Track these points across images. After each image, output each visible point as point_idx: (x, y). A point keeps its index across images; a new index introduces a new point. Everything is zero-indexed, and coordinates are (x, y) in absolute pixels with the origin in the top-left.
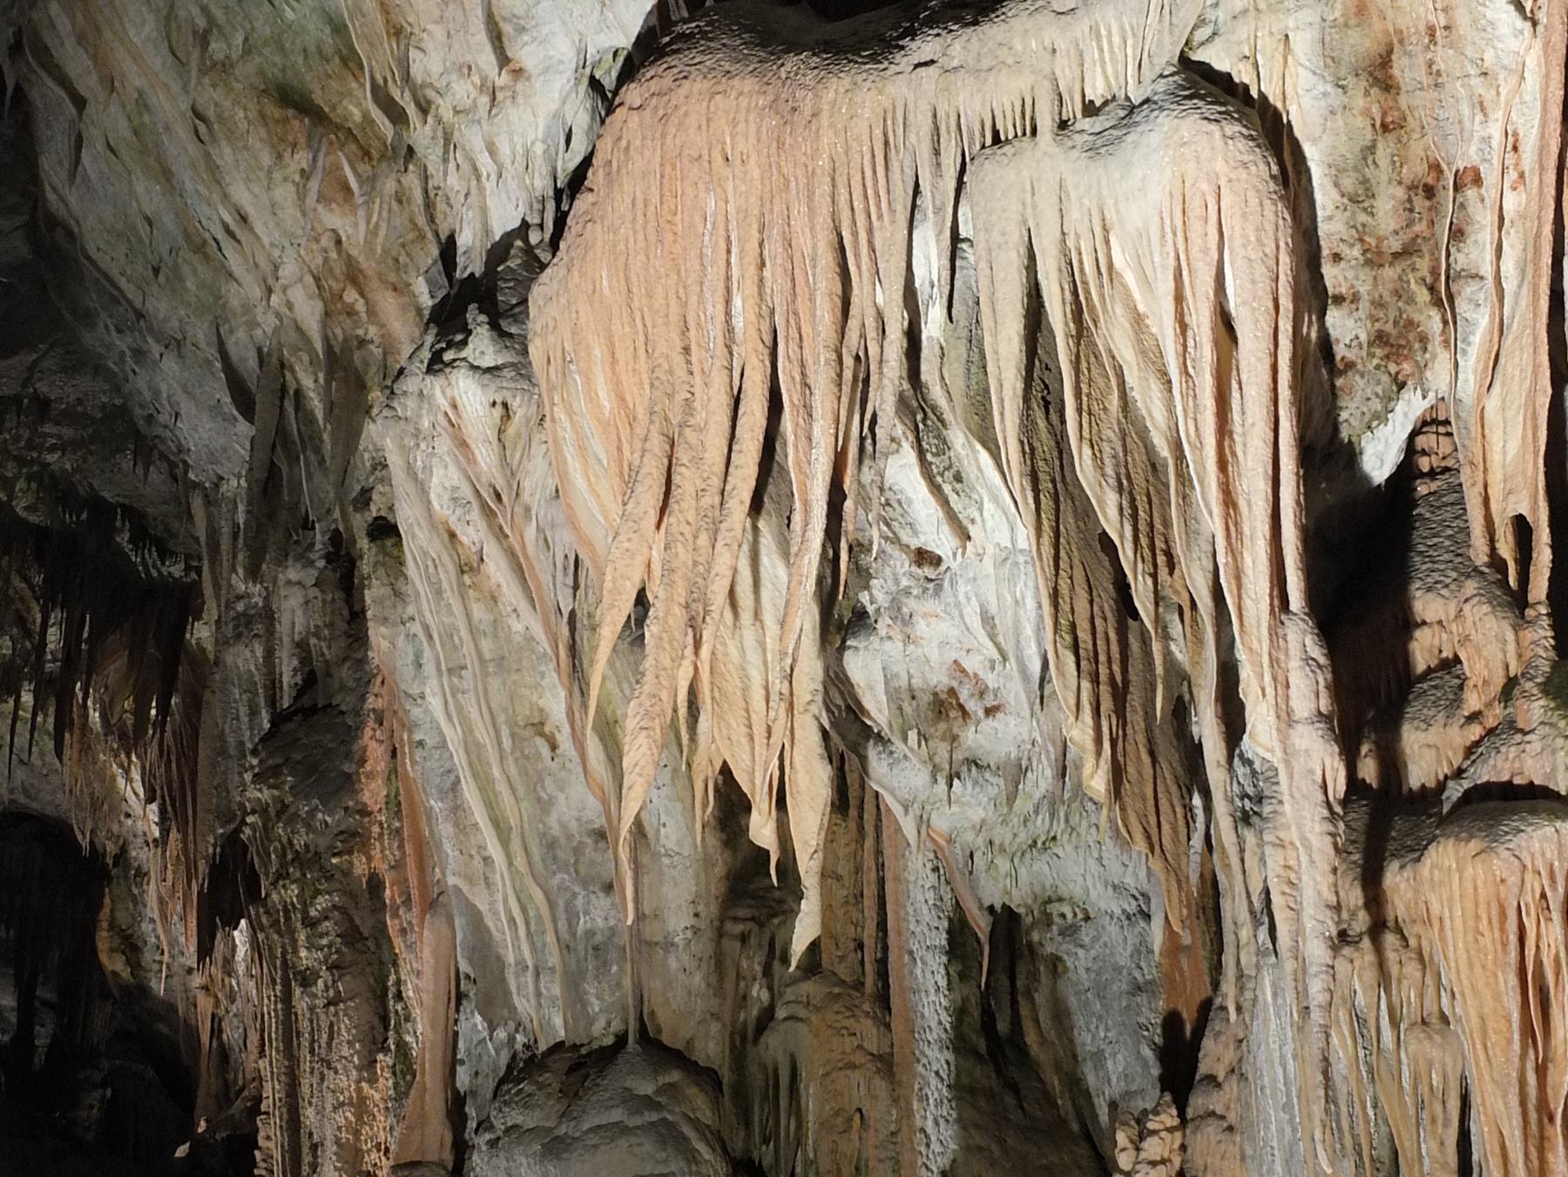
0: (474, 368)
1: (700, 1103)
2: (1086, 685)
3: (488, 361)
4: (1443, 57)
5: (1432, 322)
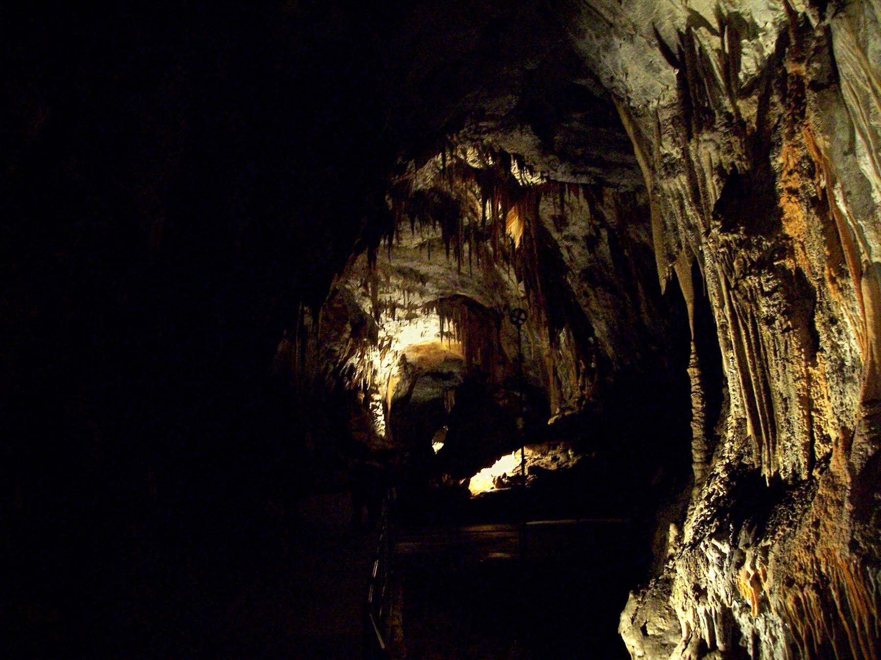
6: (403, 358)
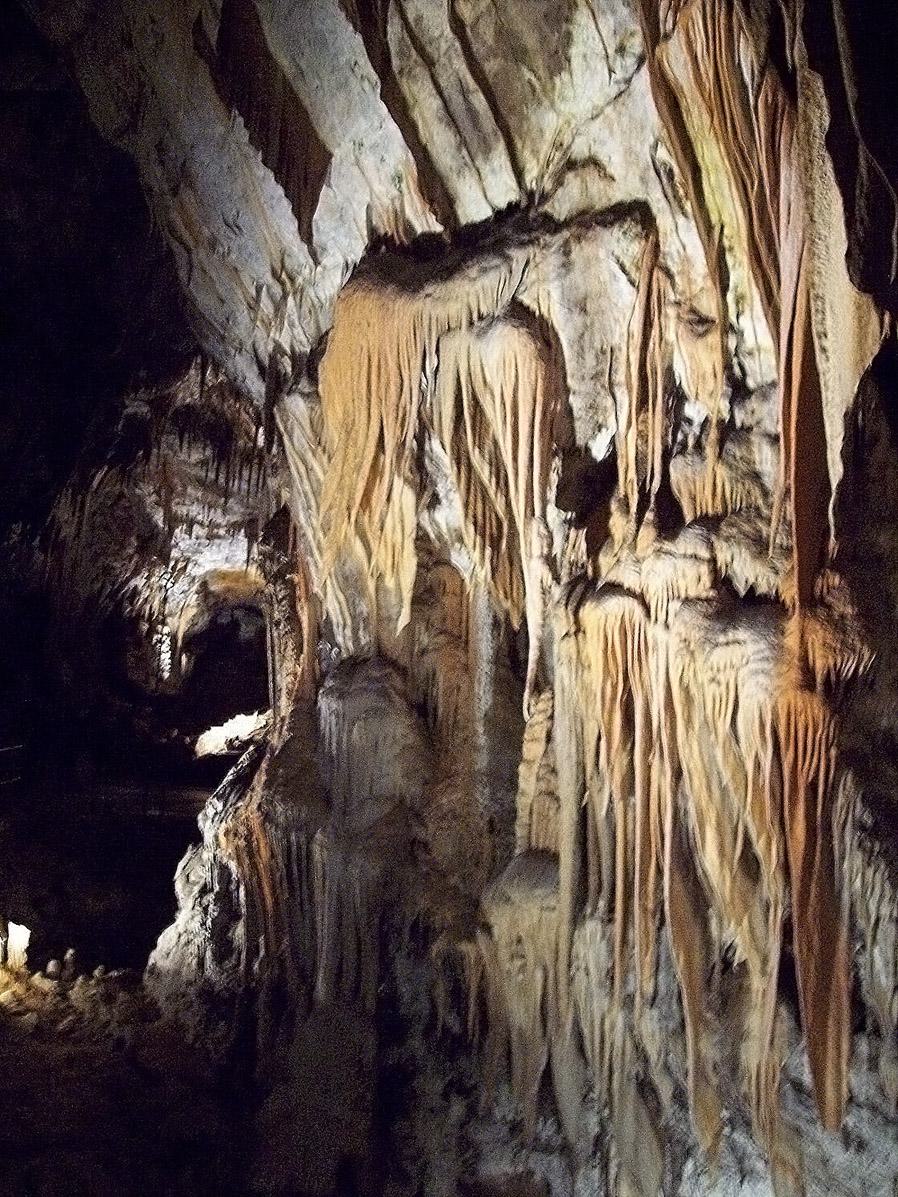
0: (303, 395)
1: (398, 681)
2: (478, 538)
3: (306, 390)
4: (604, 303)
5: (609, 401)
6: (204, 584)
